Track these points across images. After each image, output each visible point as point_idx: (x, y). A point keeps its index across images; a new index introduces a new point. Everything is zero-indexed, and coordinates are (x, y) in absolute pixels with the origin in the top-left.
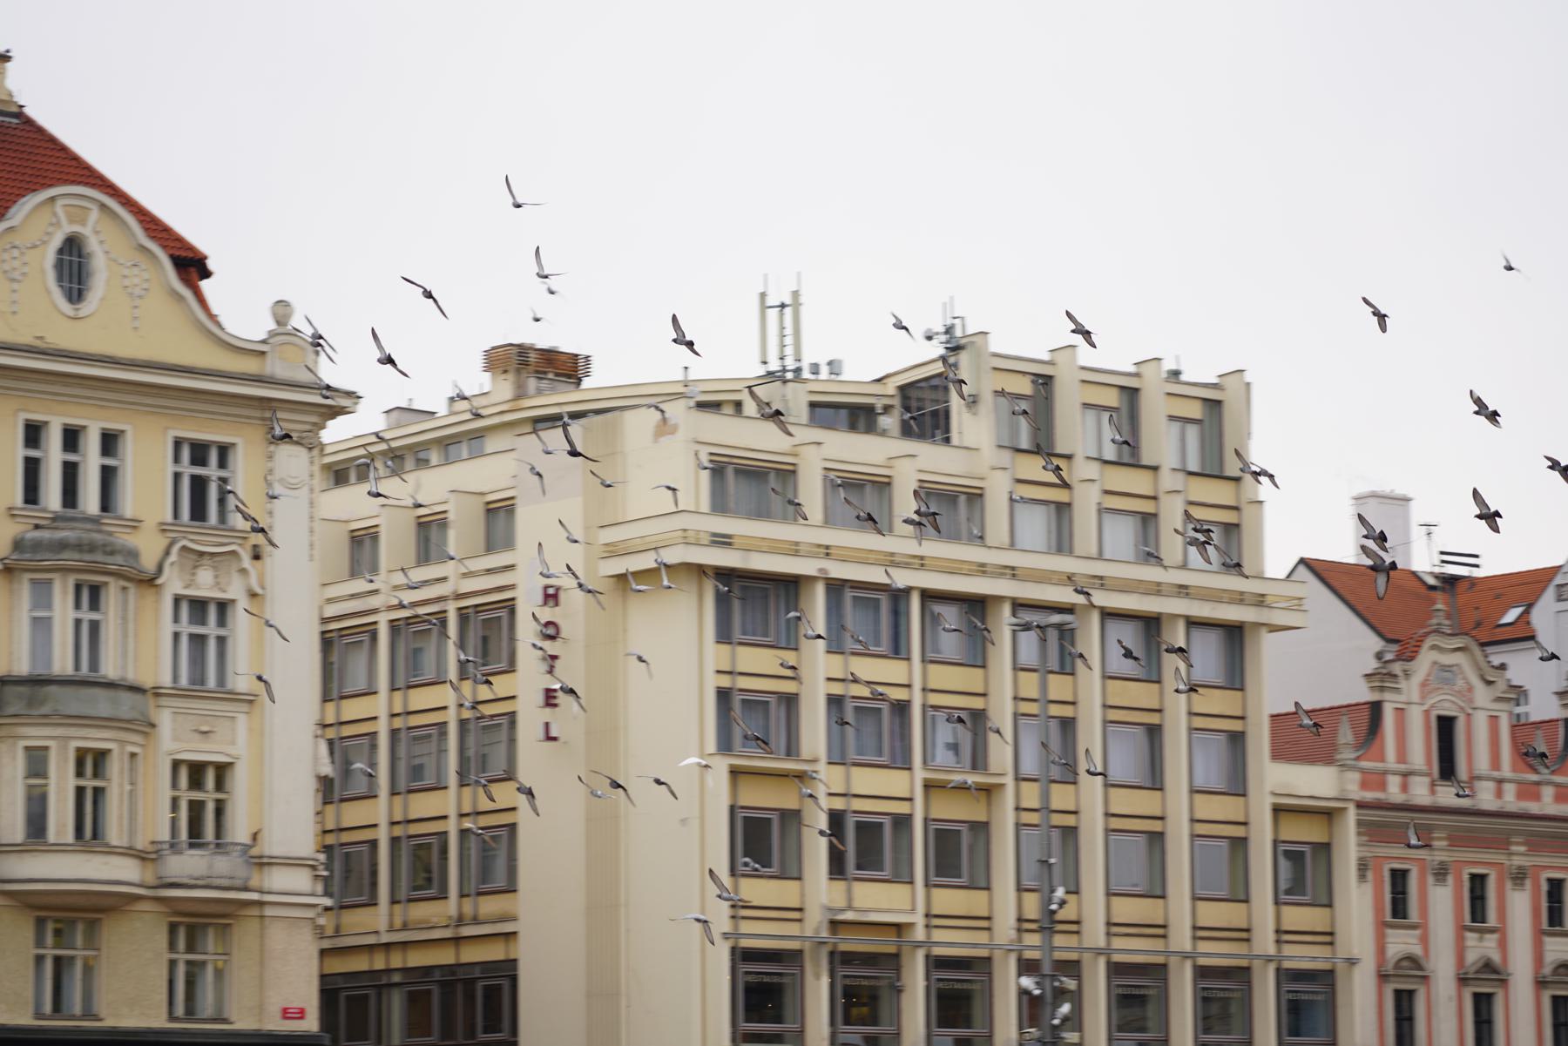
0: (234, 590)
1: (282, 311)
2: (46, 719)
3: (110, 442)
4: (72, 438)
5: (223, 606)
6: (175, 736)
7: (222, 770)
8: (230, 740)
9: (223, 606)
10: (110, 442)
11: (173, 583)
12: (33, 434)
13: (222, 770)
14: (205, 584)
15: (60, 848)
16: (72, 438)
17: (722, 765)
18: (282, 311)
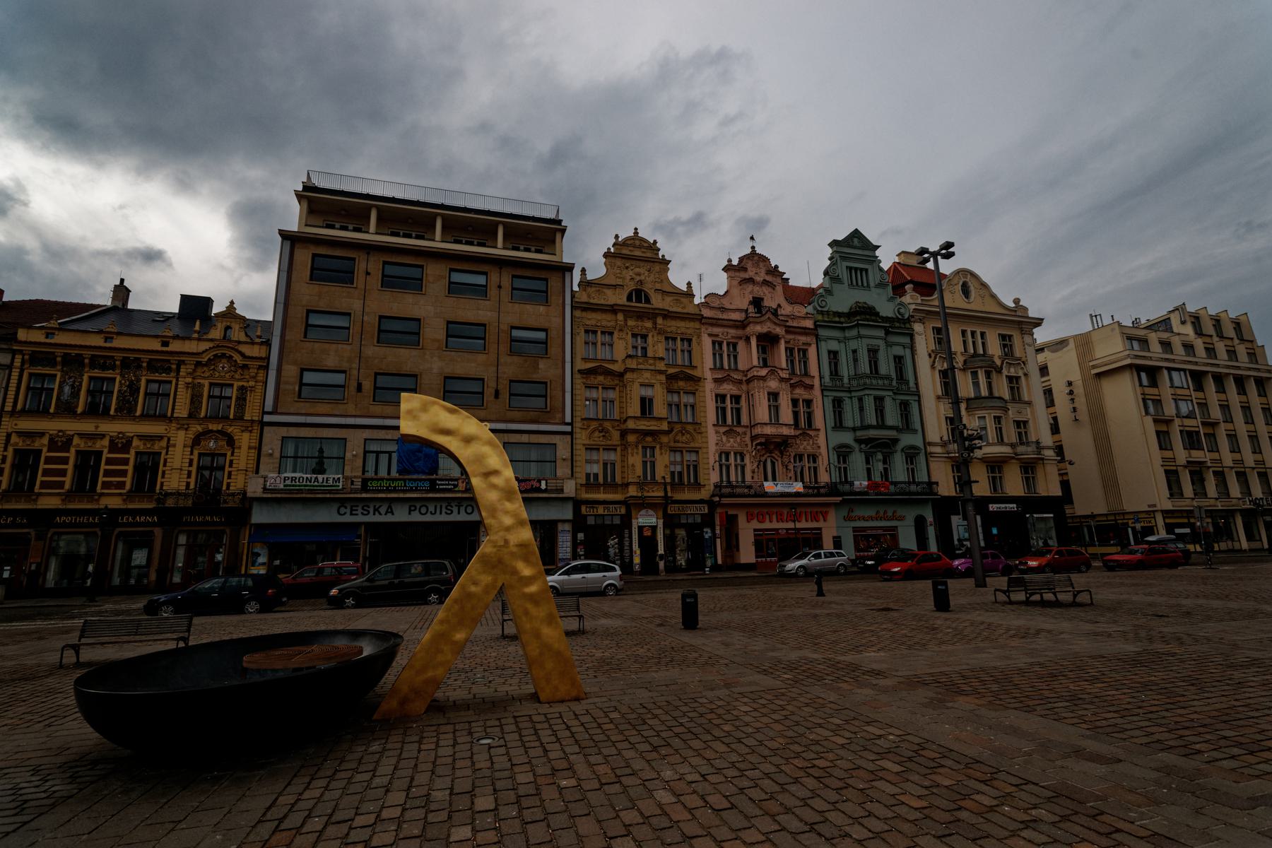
0: (1020, 374)
1: (1017, 301)
2: (985, 408)
3: (983, 334)
4: (973, 333)
5: (1018, 378)
6: (1012, 414)
7: (1025, 423)
8: (1027, 414)
9: (1018, 378)
10: (983, 334)
11: (1005, 372)
12: (964, 332)
13: (1025, 423)
14: (1012, 372)
15: (992, 444)
16: (973, 333)
17: (1149, 420)
18: (1017, 301)
